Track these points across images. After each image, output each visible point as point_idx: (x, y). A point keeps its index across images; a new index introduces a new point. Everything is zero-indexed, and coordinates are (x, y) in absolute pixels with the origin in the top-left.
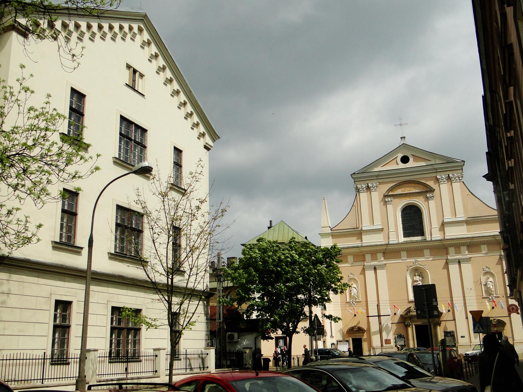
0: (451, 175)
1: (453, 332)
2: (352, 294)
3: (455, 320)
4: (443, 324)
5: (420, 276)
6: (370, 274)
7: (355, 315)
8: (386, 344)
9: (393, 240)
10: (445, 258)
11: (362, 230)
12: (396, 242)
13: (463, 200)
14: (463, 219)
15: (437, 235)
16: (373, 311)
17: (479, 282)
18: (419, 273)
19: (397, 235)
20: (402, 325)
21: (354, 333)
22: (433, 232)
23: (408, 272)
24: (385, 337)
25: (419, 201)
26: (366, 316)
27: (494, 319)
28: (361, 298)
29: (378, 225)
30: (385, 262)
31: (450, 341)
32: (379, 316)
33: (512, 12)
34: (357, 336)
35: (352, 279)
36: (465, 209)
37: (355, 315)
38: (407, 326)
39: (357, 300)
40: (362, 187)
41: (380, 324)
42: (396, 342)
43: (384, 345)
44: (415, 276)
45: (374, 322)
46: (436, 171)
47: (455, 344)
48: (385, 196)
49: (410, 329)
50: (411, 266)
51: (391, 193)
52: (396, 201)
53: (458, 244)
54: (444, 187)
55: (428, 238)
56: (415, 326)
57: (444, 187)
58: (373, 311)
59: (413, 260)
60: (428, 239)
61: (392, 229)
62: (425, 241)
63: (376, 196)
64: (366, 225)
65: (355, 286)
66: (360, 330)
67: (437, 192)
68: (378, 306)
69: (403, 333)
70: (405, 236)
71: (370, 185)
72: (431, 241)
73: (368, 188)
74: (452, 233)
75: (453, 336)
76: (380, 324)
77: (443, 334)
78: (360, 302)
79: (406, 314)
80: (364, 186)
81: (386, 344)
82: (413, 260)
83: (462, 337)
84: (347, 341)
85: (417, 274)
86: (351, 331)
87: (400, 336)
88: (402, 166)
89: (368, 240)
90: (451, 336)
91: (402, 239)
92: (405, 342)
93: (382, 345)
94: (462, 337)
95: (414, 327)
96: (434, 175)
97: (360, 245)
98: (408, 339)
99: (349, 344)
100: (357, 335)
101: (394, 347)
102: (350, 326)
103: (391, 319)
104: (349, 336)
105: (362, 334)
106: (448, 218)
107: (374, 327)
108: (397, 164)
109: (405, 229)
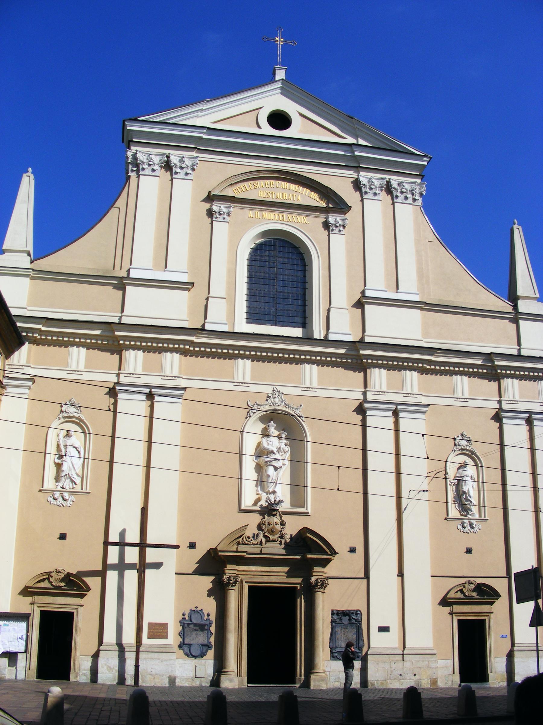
0: (394, 184)
1: (357, 612)
3: (367, 576)
9: (217, 320)
11: (128, 277)
12: (225, 328)
13: (418, 252)
14: (417, 298)
15: (344, 328)
17: (442, 475)
19: (229, 311)
22: (335, 317)
25: (305, 228)
26: (102, 541)
27: (470, 583)
29: (179, 269)
33: (293, 186)
34: (61, 603)
36: (421, 275)
40: (150, 160)
46: (355, 164)
48: (210, 198)
49: (233, 596)
51: (230, 192)
52: (240, 213)
53: (401, 358)
54: (376, 208)
55: (318, 333)
57: (376, 208)
59: (269, 390)
60: (316, 336)
61: (218, 287)
62: (308, 339)
63: (186, 194)
64: (143, 265)
67: (352, 216)
68: (144, 511)
70: (253, 316)
71: (174, 160)
72: (326, 342)
73: (168, 166)
74: (387, 326)
77: (329, 618)
80: (156, 160)
83: (384, 629)
88: (267, 130)
89: (144, 307)
90: (351, 624)
91: (242, 326)
94: (384, 629)
95: (246, 587)
96: (351, 173)
97: (116, 320)
106: (377, 286)
108: (259, 127)
109: (252, 296)
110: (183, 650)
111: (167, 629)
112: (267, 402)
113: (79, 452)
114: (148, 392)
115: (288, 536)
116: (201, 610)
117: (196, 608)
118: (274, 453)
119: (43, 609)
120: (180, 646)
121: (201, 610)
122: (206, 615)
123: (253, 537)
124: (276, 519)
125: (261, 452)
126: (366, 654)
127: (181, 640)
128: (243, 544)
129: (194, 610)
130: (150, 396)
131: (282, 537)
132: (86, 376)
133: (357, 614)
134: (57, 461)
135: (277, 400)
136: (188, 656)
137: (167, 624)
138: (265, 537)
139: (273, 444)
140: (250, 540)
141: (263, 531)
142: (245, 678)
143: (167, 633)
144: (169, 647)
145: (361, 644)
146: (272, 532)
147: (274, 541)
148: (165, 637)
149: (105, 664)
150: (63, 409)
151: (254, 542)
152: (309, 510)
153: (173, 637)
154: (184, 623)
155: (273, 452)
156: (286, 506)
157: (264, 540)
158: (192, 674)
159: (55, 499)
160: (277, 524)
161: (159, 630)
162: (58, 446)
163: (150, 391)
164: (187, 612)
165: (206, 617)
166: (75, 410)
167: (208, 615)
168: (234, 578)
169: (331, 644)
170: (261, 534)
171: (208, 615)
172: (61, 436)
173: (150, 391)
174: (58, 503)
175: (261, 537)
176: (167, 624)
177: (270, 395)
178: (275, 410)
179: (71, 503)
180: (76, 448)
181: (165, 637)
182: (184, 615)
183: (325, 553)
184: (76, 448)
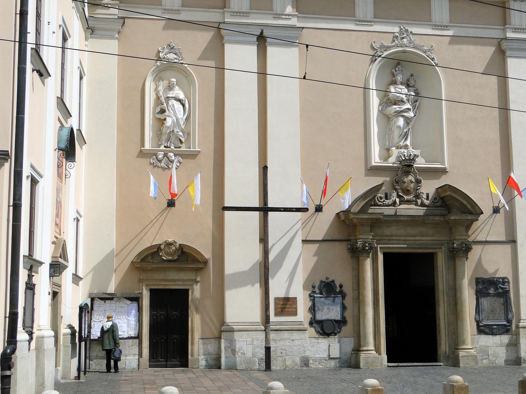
1: (504, 281)
2: (169, 122)
4: (476, 251)
5: (408, 86)
6: (240, 56)
7: (171, 204)
8: (276, 315)
10: (496, 33)
16: (241, 189)
18: (408, 75)
20: (340, 250)
21: (165, 269)
23: (375, 66)
24: (277, 290)
28: (200, 142)
30: (294, 22)
31: (493, 311)
32: (264, 210)
34: (173, 280)
35: (171, 66)
37: (171, 204)
38: (356, 253)
39: (183, 148)
41: (264, 239)
42: (313, 309)
43: (273, 318)
44: (394, 83)
45: (240, 232)
47: (509, 321)
49: (368, 264)
50: (388, 48)
56: (385, 255)
58: (241, 189)
59: (396, 29)
65: (182, 96)
66: (185, 258)
69: (342, 277)
75: (505, 294)
76: (264, 239)
78: (193, 155)
79: (363, 210)
81: (276, 315)
82: (396, 29)
84: (136, 299)
85: (399, 78)
86: (150, 260)
87: (327, 289)
92: (344, 308)
93: (266, 320)
98: (359, 300)
99: (140, 310)
100: (173, 275)
101: (306, 325)
102: (147, 243)
103: (305, 224)
104: (141, 281)
105: (190, 275)
107: (240, 252)
110: (315, 327)
111: (296, 303)
112: (394, 44)
113: (184, 105)
114: (259, 34)
115: (425, 196)
116: (333, 281)
117: (327, 278)
118: (403, 102)
119: (153, 287)
120: (311, 324)
121: (333, 281)
122: (338, 286)
123: (386, 198)
124: (411, 178)
125: (387, 101)
126: (518, 327)
127: (311, 316)
128: (375, 205)
129: (325, 282)
130: (262, 40)
131: (417, 196)
132: (183, 16)
133: (504, 283)
134: (159, 116)
135: (405, 40)
136: (321, 334)
137: (296, 298)
138: (399, 196)
139: (400, 91)
140: (382, 200)
141: (396, 190)
142: (385, 357)
143: (296, 308)
144: (300, 323)
145: (510, 316)
146: (407, 192)
147: (409, 202)
148: (295, 314)
149: (229, 347)
150: (161, 55)
151: (387, 202)
152: (446, 165)
153: (303, 314)
154: (314, 297)
155: (402, 102)
156: (420, 163)
157: (398, 200)
158: (325, 355)
159: (160, 161)
160: (412, 182)
161: (287, 305)
162: (158, 98)
163: (262, 33)
164: (317, 284)
165: (338, 290)
166: (175, 56)
167: (341, 286)
168: (369, 244)
169: (477, 316)
170: (395, 194)
171: (341, 286)
172: (161, 88)
173: (262, 33)
174: (163, 164)
175: (394, 197)
176: (296, 298)
177: (397, 34)
178: (404, 52)
179: (178, 164)
180: (180, 101)
181: (295, 314)
182: (314, 287)
183: (471, 213)
184: (180, 101)
